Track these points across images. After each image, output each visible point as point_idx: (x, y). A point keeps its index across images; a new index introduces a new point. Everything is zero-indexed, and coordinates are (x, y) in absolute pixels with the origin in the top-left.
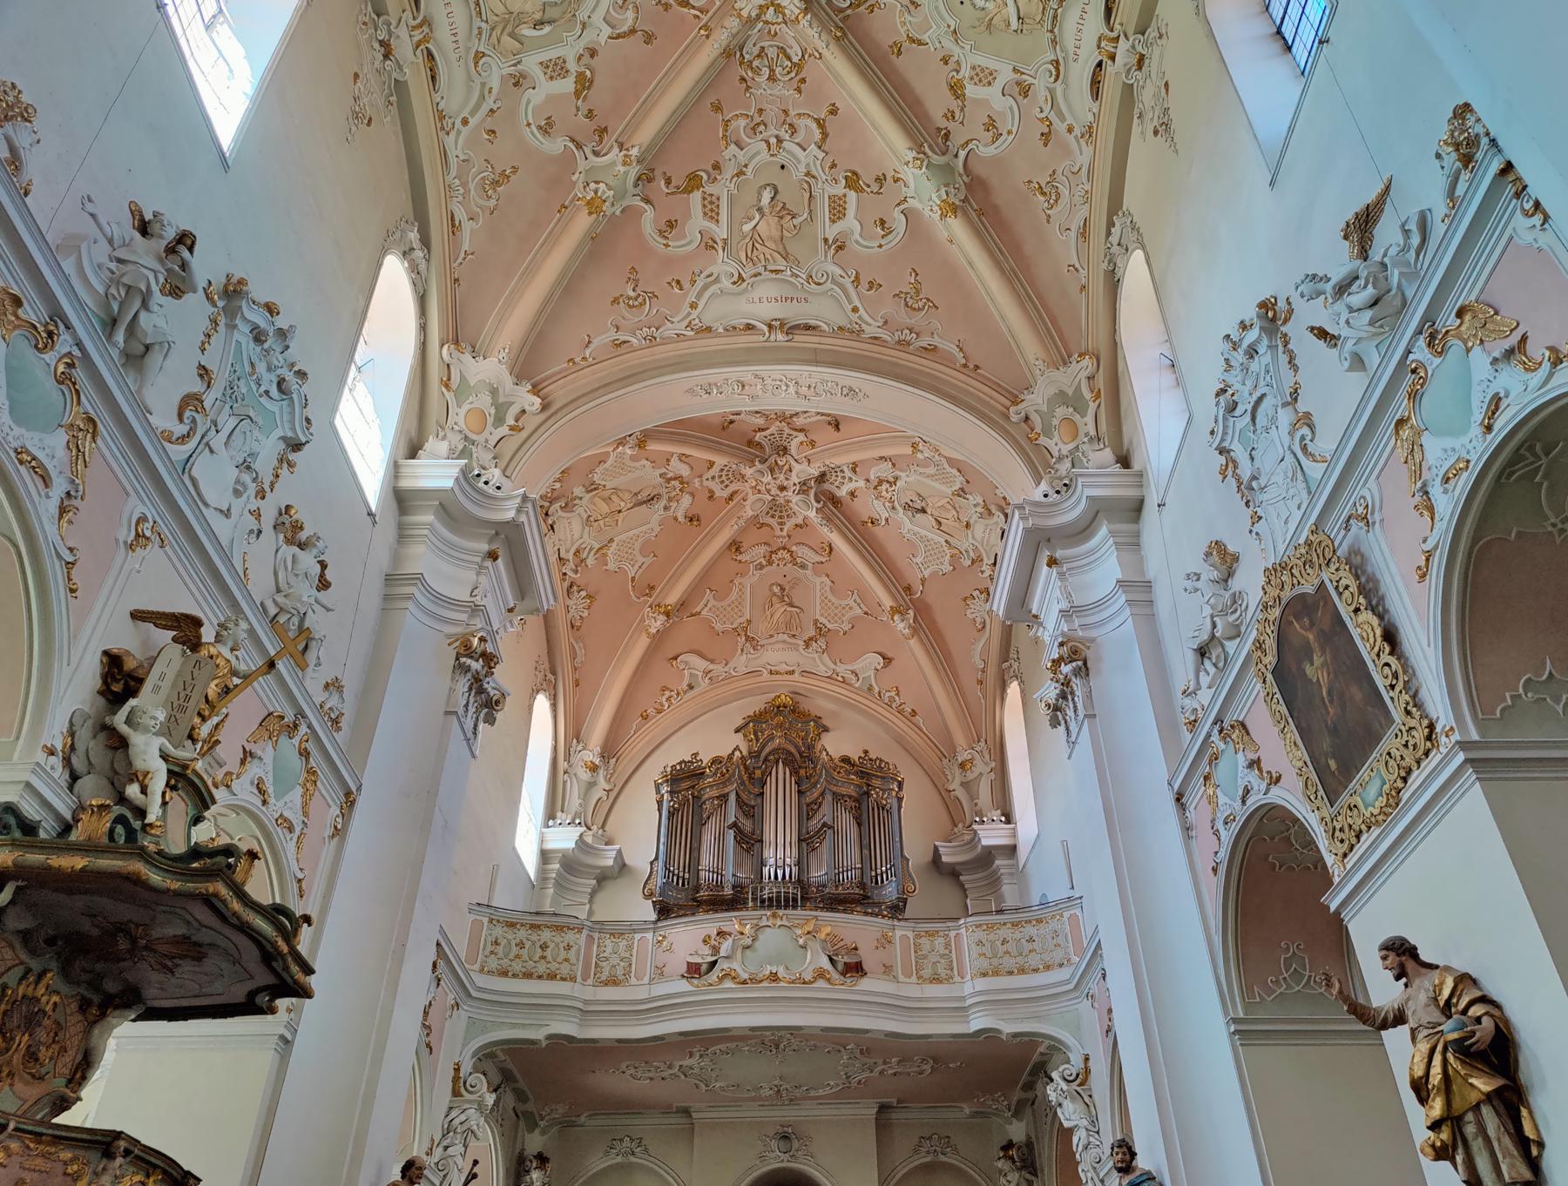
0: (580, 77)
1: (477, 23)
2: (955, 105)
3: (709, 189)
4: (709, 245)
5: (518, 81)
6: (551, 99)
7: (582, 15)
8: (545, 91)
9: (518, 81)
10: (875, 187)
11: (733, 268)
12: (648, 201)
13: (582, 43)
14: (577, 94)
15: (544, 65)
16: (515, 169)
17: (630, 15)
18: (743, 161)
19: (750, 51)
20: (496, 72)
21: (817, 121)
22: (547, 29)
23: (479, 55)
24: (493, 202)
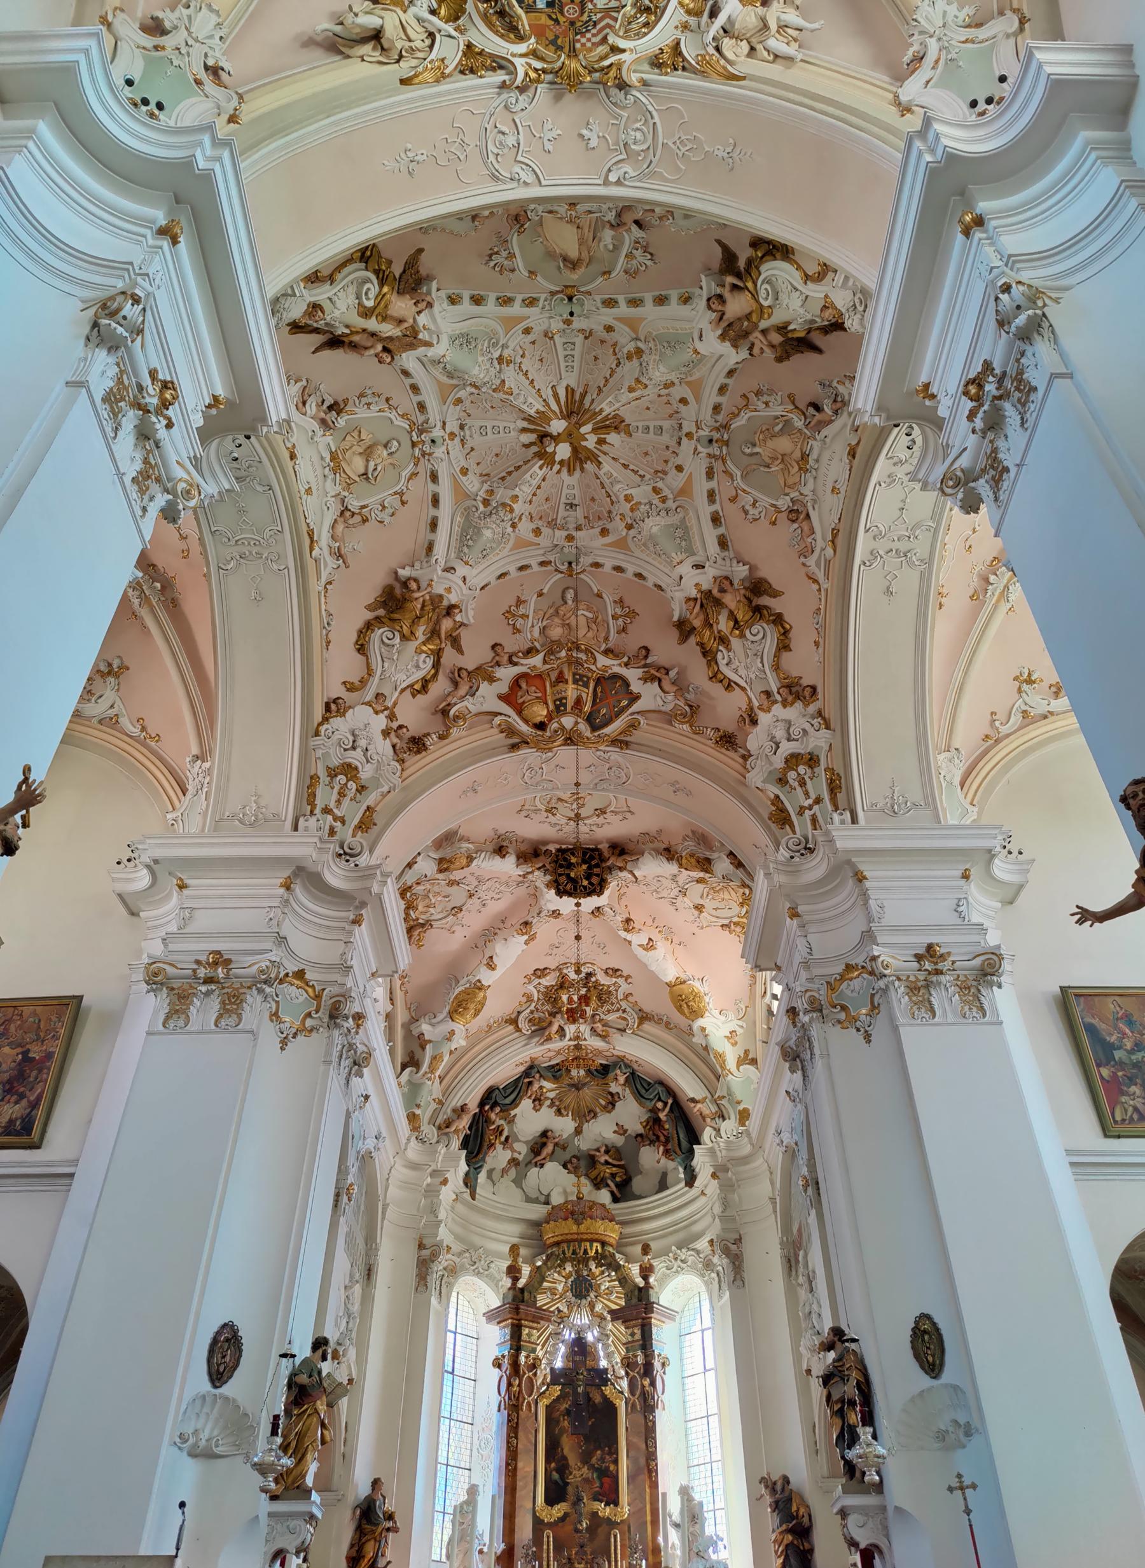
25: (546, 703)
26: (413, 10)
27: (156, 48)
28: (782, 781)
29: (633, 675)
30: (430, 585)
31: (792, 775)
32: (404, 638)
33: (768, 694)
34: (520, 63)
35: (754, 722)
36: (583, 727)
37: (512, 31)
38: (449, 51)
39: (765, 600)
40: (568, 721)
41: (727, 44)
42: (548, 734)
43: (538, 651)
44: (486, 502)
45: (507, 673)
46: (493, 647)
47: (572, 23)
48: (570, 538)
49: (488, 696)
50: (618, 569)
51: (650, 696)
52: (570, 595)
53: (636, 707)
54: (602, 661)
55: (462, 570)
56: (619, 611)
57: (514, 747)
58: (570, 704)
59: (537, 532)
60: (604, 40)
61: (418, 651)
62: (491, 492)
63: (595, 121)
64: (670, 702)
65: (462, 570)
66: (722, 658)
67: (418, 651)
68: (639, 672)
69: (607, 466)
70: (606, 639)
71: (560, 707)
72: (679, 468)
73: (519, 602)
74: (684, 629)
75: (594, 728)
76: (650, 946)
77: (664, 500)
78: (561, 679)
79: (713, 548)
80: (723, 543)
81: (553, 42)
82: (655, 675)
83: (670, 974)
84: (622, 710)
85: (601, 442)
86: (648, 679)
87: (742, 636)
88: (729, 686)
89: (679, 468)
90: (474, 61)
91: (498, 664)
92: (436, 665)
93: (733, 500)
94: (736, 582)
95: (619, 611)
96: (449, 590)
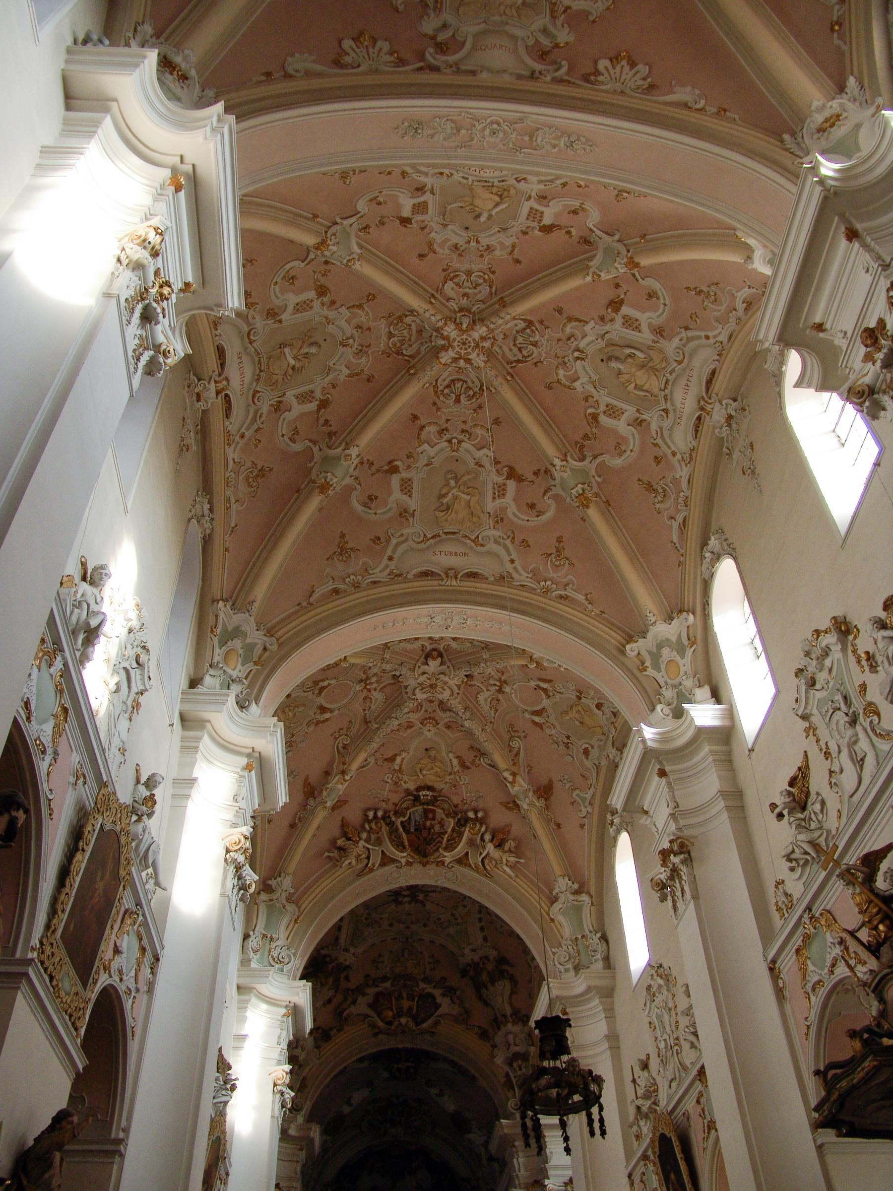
0: (617, 310)
1: (671, 378)
2: (323, 281)
3: (535, 224)
4: (543, 198)
5: (659, 332)
6: (643, 310)
7: (601, 344)
8: (645, 318)
9: (659, 332)
10: (385, 220)
11: (522, 186)
12: (591, 230)
13: (607, 328)
14: (622, 302)
15: (638, 329)
16: (688, 288)
17: (568, 330)
18: (501, 235)
19: (485, 290)
20: (670, 346)
21: (435, 252)
22: (628, 351)
23: (680, 363)
24: (713, 288)
25: (392, 1010)
26: (362, 843)
27: (271, 900)
28: (510, 1065)
29: (437, 993)
30: (336, 959)
31: (515, 1065)
32: (322, 984)
33: (505, 1016)
34: (403, 861)
35: (499, 1028)
36: (412, 1024)
37: (400, 846)
38: (376, 859)
39: (505, 967)
40: (403, 1020)
41: (486, 861)
42: (393, 1028)
43: (389, 979)
44: (366, 919)
45: (372, 991)
46: (367, 976)
47: (425, 839)
48: (408, 927)
49: (362, 1006)
50: (432, 942)
51: (445, 1006)
52: (406, 952)
53: (437, 1013)
54: (422, 985)
55: (352, 950)
56: (431, 960)
57: (376, 1035)
58: (405, 1009)
59: (391, 925)
60: (437, 849)
61: (329, 990)
62: (369, 914)
63: (432, 869)
64: (456, 1010)
65: (352, 950)
66: (484, 992)
67: (329, 990)
68: (441, 991)
69: (429, 906)
70: (424, 973)
71: (400, 1013)
72: (465, 906)
73: (380, 956)
74: (464, 973)
75: (417, 1025)
76: (441, 1094)
77: (456, 919)
78: (400, 997)
79: (480, 941)
80: (485, 939)
81: (417, 849)
82: (449, 991)
83: (451, 1107)
84: (432, 1015)
85: (426, 896)
86: (444, 995)
87: (493, 985)
88: (486, 1004)
89: (465, 906)
90: (386, 860)
91: (368, 986)
92: (336, 992)
93: (491, 923)
94: (491, 958)
95: (431, 960)
96: (345, 960)
